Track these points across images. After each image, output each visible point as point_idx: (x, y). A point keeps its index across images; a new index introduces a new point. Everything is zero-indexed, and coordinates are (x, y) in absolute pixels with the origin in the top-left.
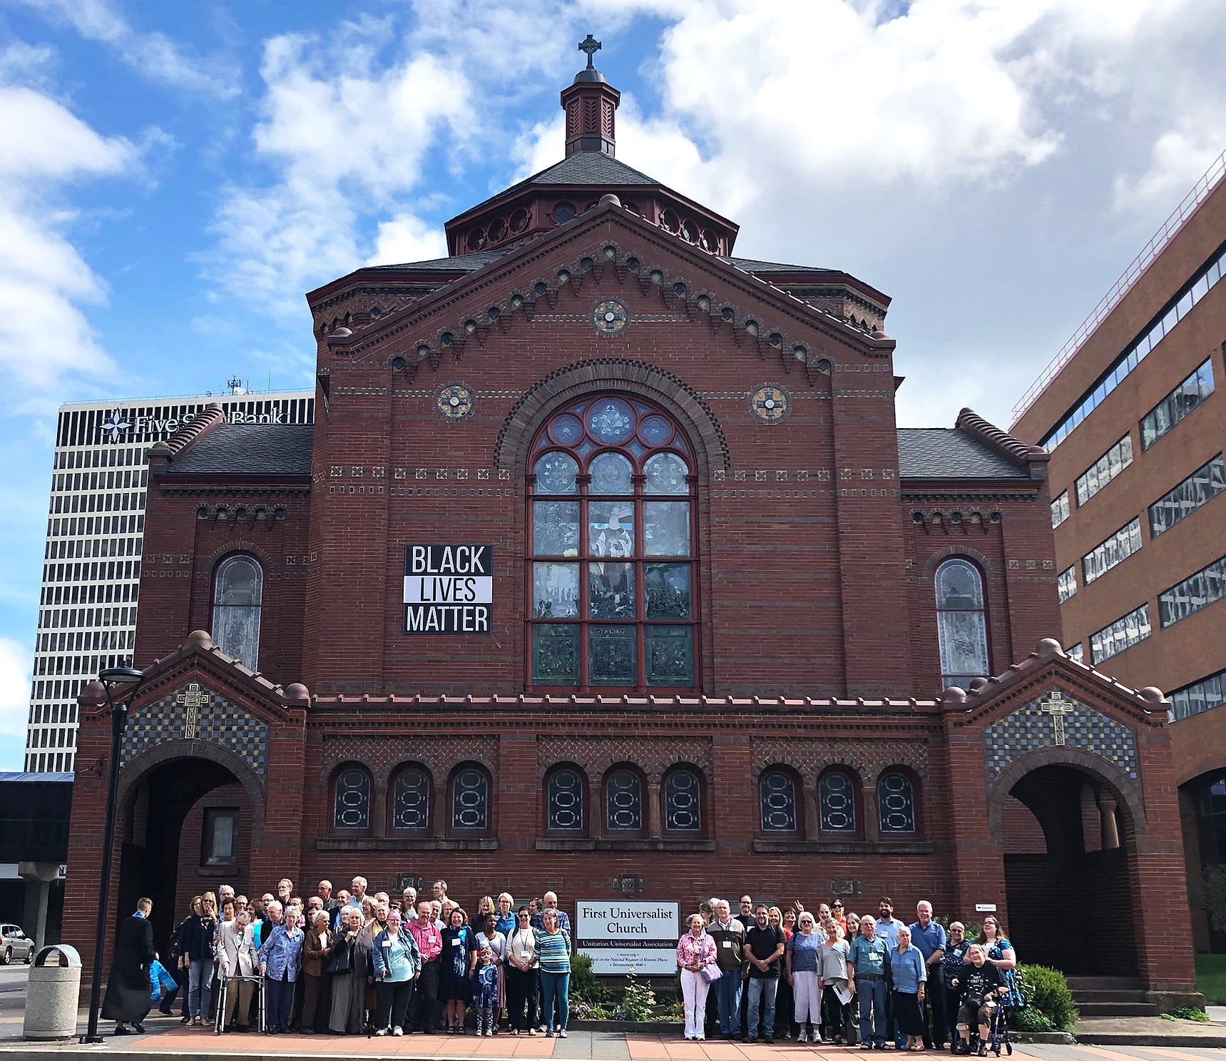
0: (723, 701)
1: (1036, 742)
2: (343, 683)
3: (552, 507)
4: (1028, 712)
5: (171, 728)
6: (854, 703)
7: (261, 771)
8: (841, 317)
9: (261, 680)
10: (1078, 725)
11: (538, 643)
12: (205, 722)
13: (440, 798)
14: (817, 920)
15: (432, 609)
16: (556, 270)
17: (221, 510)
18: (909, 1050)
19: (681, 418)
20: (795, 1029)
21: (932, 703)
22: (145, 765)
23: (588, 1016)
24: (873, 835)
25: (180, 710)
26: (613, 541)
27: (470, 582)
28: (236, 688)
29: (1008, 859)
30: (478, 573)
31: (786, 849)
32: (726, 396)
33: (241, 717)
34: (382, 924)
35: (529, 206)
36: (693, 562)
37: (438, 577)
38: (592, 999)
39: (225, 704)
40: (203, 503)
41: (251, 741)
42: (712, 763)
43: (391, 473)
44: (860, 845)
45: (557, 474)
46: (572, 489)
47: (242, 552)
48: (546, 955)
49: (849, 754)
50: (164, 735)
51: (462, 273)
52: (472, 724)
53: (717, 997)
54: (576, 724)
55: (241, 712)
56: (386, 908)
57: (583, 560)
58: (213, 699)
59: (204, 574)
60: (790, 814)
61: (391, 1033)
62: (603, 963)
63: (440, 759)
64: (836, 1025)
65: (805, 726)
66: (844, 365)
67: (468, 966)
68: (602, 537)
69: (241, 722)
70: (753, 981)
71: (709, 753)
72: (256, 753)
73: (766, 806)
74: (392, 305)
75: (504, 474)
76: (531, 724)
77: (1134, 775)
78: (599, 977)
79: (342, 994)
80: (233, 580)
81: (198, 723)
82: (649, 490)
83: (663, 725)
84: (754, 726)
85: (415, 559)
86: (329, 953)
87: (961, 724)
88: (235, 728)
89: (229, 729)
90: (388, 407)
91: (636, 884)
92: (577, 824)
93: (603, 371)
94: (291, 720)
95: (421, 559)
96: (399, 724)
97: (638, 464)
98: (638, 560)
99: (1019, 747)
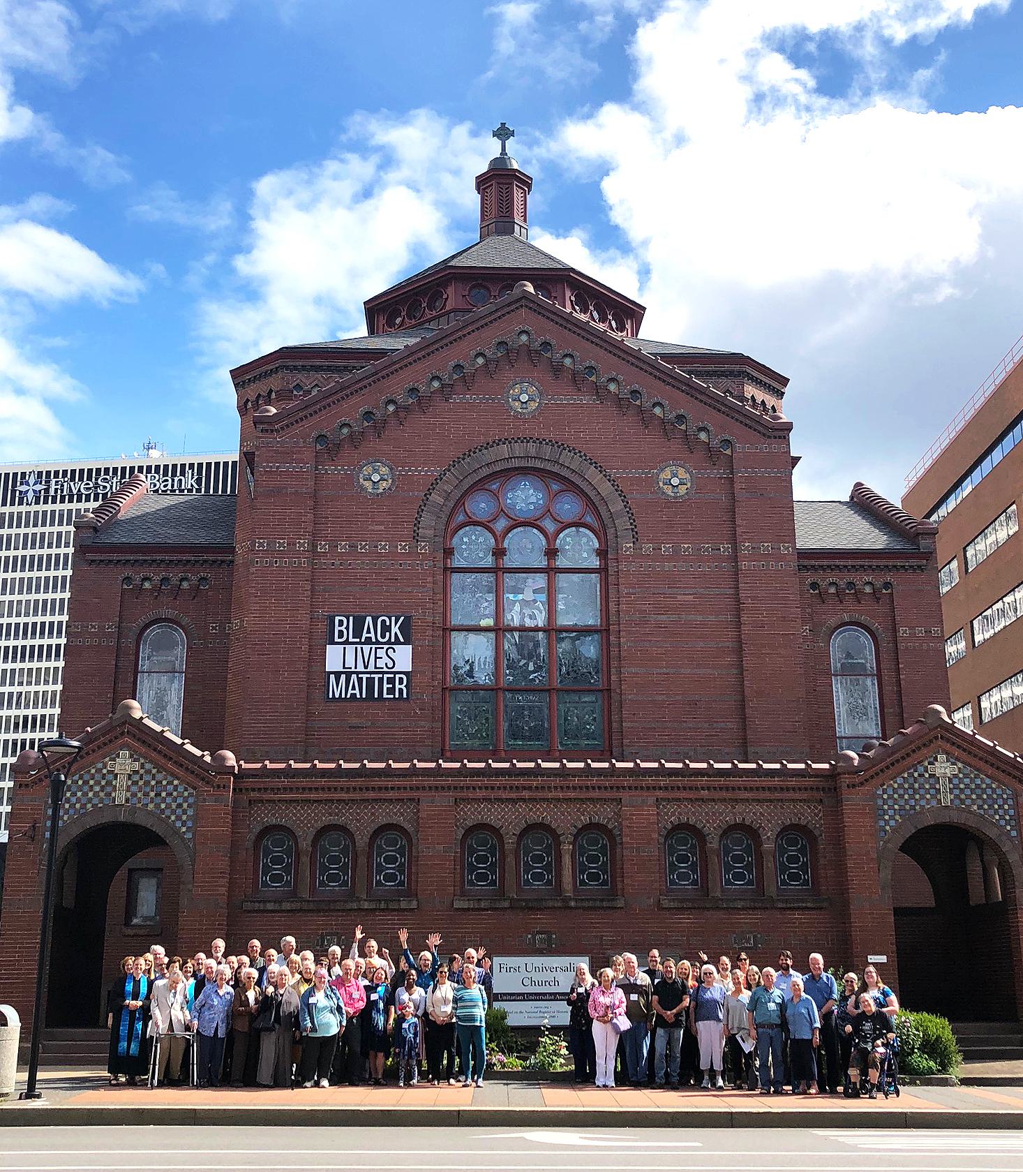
0: (631, 765)
1: (923, 803)
2: (266, 749)
3: (470, 578)
4: (916, 775)
5: (102, 794)
6: (754, 766)
7: (189, 835)
8: (742, 398)
9: (189, 747)
10: (962, 786)
11: (455, 708)
12: (134, 789)
13: (362, 860)
14: (719, 972)
15: (354, 676)
16: (473, 353)
17: (145, 579)
18: (804, 1093)
19: (592, 494)
20: (699, 1076)
21: (826, 766)
23: (504, 1066)
24: (771, 890)
25: (110, 777)
26: (527, 611)
28: (165, 756)
29: (898, 912)
30: (397, 642)
31: (690, 905)
32: (634, 473)
34: (308, 981)
35: (445, 287)
36: (603, 631)
37: (359, 647)
38: (508, 1050)
39: (154, 771)
40: (128, 572)
41: (180, 806)
42: (620, 824)
44: (759, 900)
45: (472, 546)
46: (489, 561)
47: (166, 620)
48: (464, 1007)
49: (749, 813)
50: (95, 801)
51: (381, 353)
52: (392, 788)
53: (627, 1044)
54: (493, 788)
55: (170, 779)
56: (312, 967)
57: (499, 630)
58: (142, 766)
59: (130, 641)
60: (695, 872)
61: (317, 1084)
62: (519, 1015)
63: (361, 822)
64: (738, 1071)
65: (709, 789)
66: (745, 446)
67: (387, 1020)
68: (517, 607)
69: (170, 788)
70: (660, 1031)
71: (618, 814)
72: (184, 817)
73: (672, 864)
74: (315, 383)
75: (424, 548)
76: (449, 788)
77: (1014, 833)
78: (514, 1029)
79: (269, 1048)
80: (158, 646)
81: (128, 791)
82: (561, 562)
83: (574, 788)
84: (660, 788)
85: (337, 629)
86: (257, 1010)
87: (854, 786)
88: (164, 794)
92: (493, 883)
93: (518, 449)
95: (342, 628)
96: (323, 789)
97: (551, 538)
98: (552, 630)
99: (907, 807)
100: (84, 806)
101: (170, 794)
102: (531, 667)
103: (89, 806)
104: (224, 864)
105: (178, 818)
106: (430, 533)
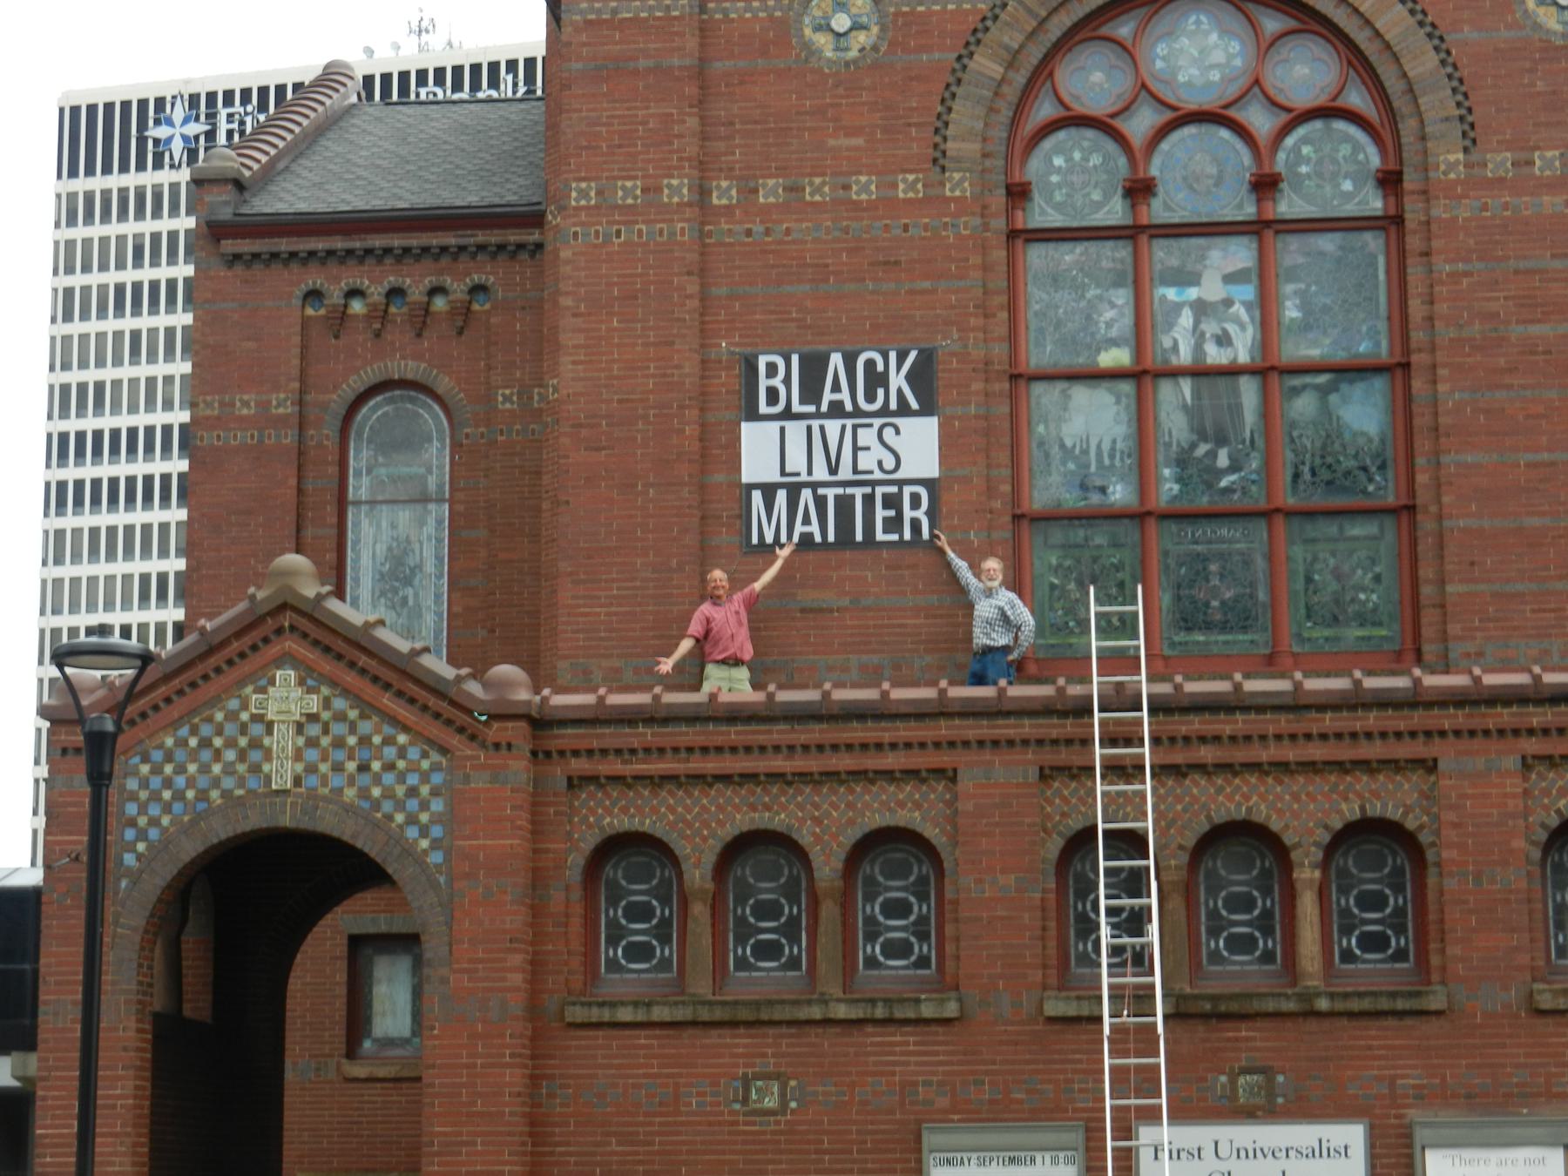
3: (1070, 255)
5: (241, 768)
7: (436, 858)
12: (312, 755)
19: (1361, 37)
22: (190, 849)
26: (1210, 328)
27: (888, 433)
28: (375, 679)
30: (904, 410)
33: (389, 741)
37: (815, 424)
42: (1437, 817)
43: (703, 192)
45: (1072, 178)
46: (1115, 212)
50: (228, 783)
55: (388, 730)
58: (327, 703)
63: (826, 825)
68: (1186, 319)
69: (389, 752)
72: (424, 818)
76: (1025, 742)
81: (298, 756)
82: (1288, 206)
83: (1324, 736)
88: (376, 766)
89: (364, 768)
90: (692, 43)
91: (1270, 1090)
94: (497, 746)
96: (734, 749)
100: (203, 795)
101: (389, 767)
102: (1223, 460)
103: (214, 794)
104: (515, 919)
105: (412, 820)
106: (974, 147)
